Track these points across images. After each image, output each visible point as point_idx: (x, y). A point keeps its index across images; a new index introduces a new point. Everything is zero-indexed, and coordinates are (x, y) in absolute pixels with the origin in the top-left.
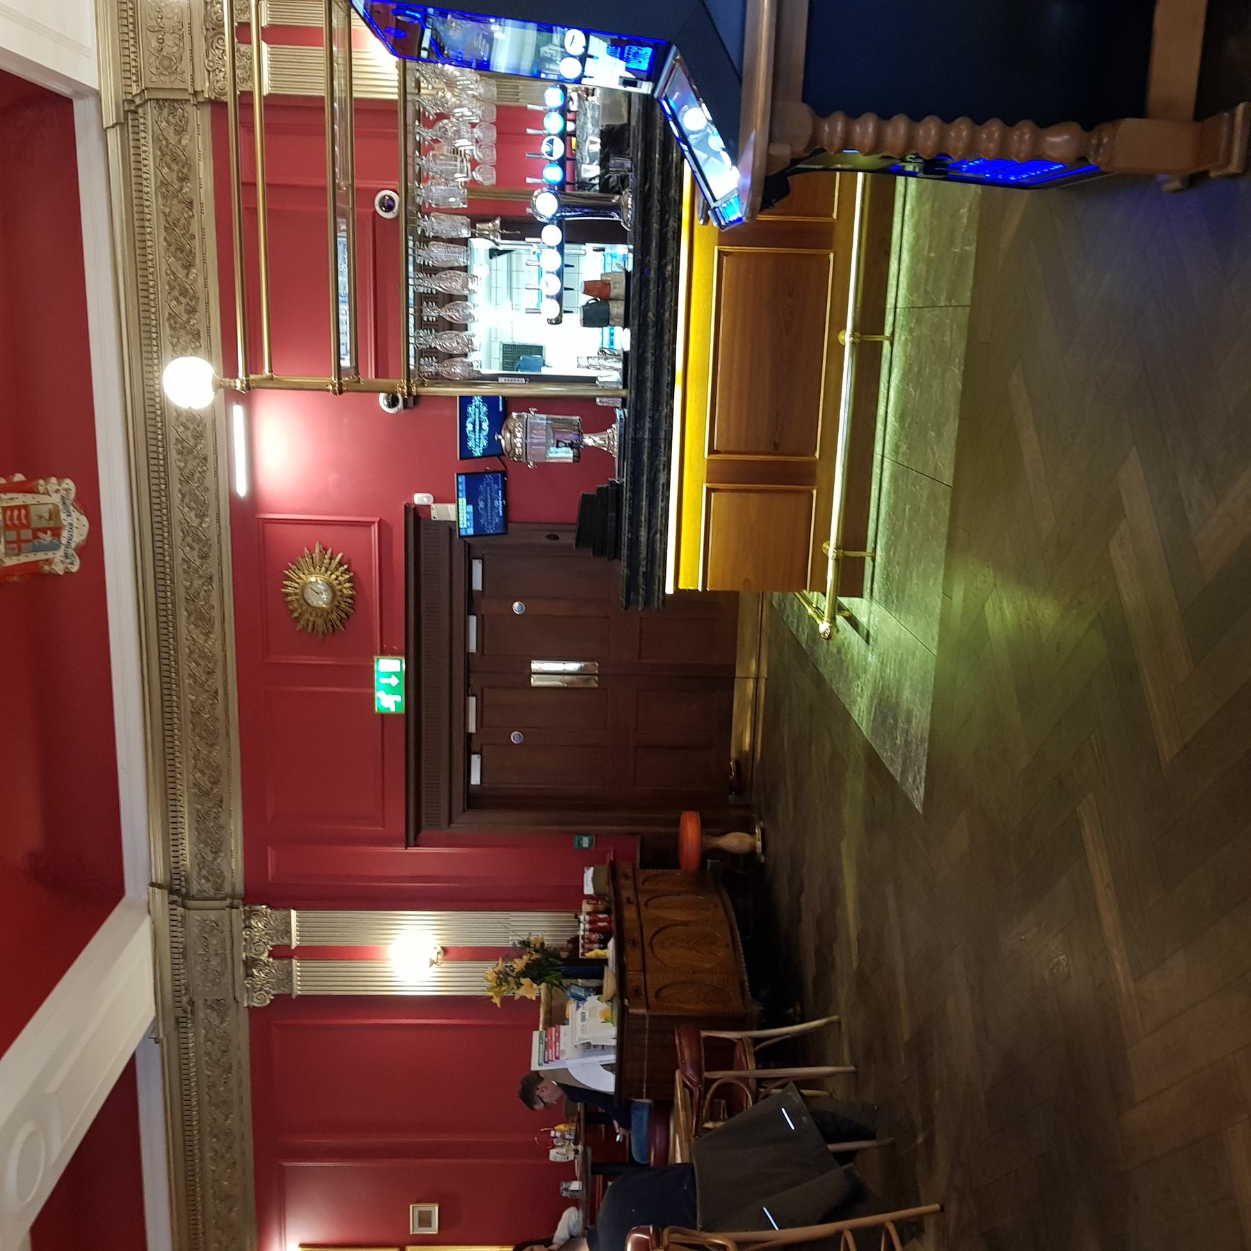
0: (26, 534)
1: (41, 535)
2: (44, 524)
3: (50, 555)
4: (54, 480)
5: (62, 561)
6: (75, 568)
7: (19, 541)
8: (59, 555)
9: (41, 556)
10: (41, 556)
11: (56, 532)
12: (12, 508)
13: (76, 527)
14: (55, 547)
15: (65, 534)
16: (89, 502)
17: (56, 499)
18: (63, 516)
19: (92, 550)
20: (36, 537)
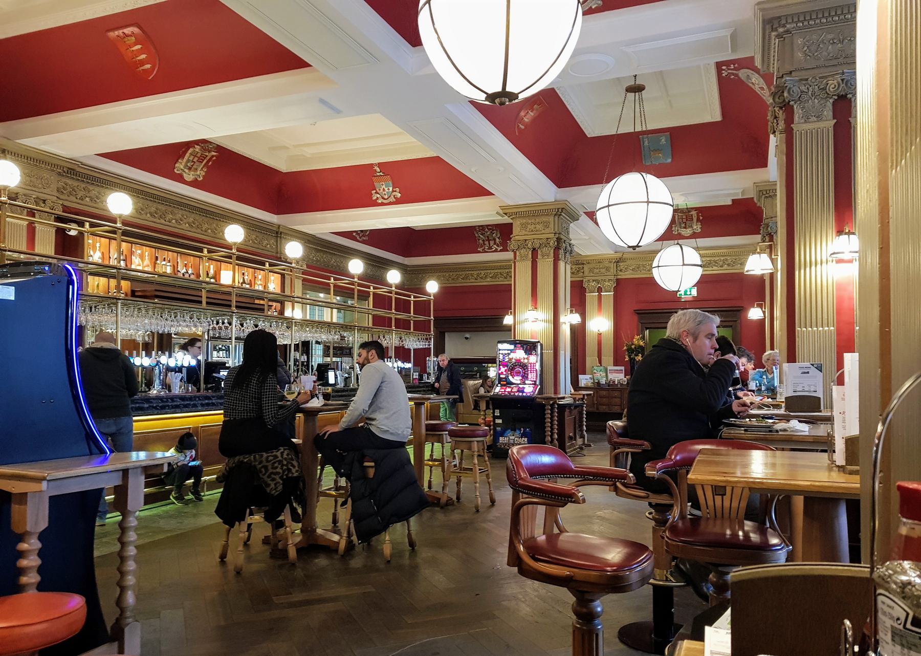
0: (195, 160)
1: (192, 163)
2: (195, 167)
3: (183, 164)
4: (204, 174)
5: (180, 166)
6: (175, 171)
7: (195, 156)
8: (182, 167)
9: (185, 160)
10: (185, 160)
11: (190, 169)
12: (205, 158)
13: (189, 177)
14: (186, 166)
15: (187, 171)
16: (195, 184)
17: (198, 173)
18: (192, 173)
19: (180, 179)
20: (193, 162)
